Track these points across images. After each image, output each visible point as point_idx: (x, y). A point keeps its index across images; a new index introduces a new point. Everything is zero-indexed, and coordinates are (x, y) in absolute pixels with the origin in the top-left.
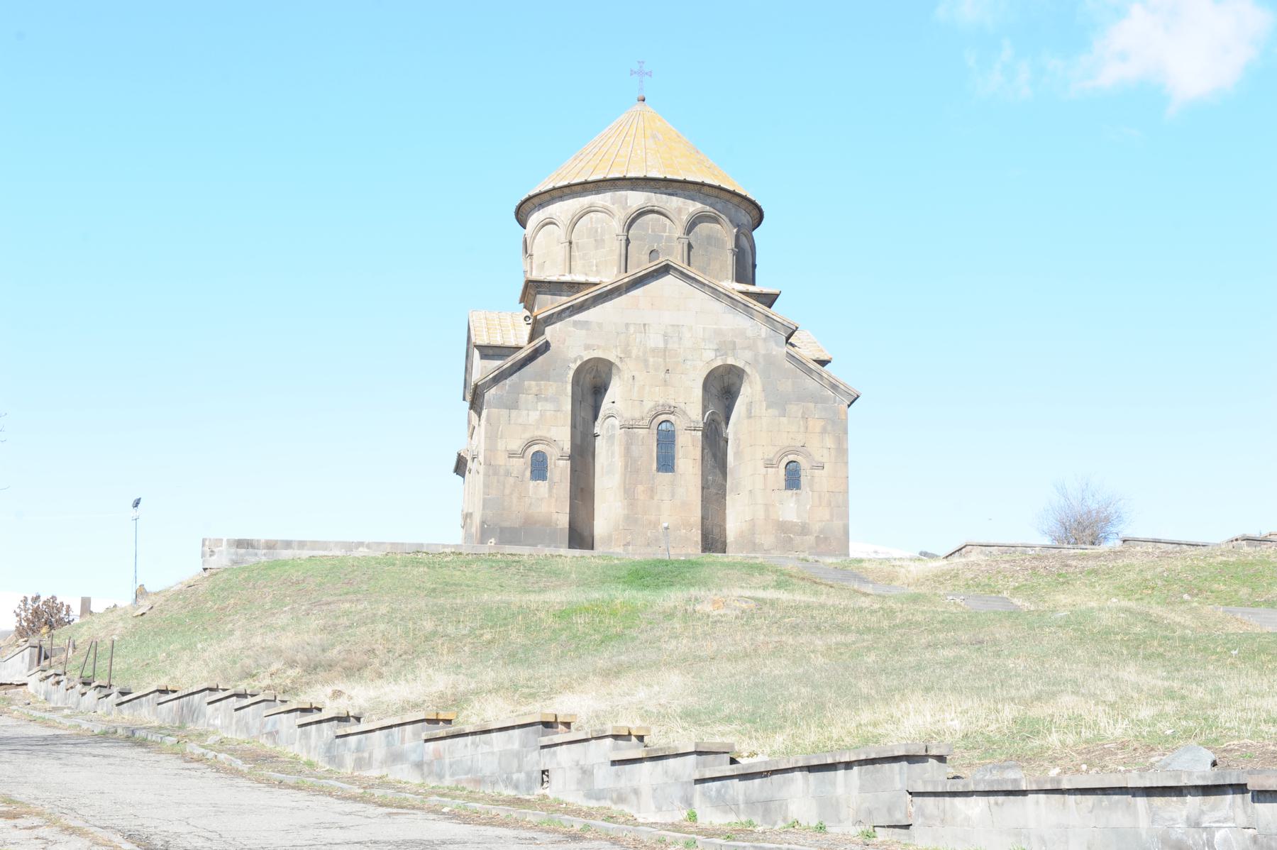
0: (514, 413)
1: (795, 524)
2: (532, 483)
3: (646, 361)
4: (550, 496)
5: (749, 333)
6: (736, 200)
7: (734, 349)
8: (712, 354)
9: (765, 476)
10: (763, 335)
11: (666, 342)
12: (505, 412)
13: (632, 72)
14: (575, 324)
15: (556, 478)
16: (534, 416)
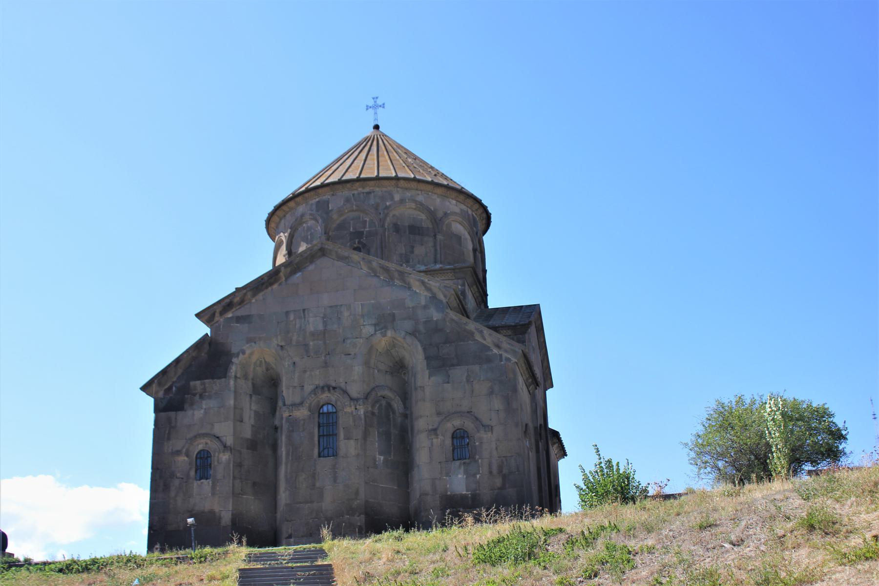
0: (180, 414)
1: (463, 497)
2: (196, 484)
3: (306, 345)
4: (213, 494)
5: (409, 303)
6: (439, 191)
7: (394, 320)
8: (370, 330)
9: (431, 450)
10: (423, 303)
11: (325, 324)
12: (172, 414)
13: (368, 107)
15: (219, 476)
16: (198, 414)
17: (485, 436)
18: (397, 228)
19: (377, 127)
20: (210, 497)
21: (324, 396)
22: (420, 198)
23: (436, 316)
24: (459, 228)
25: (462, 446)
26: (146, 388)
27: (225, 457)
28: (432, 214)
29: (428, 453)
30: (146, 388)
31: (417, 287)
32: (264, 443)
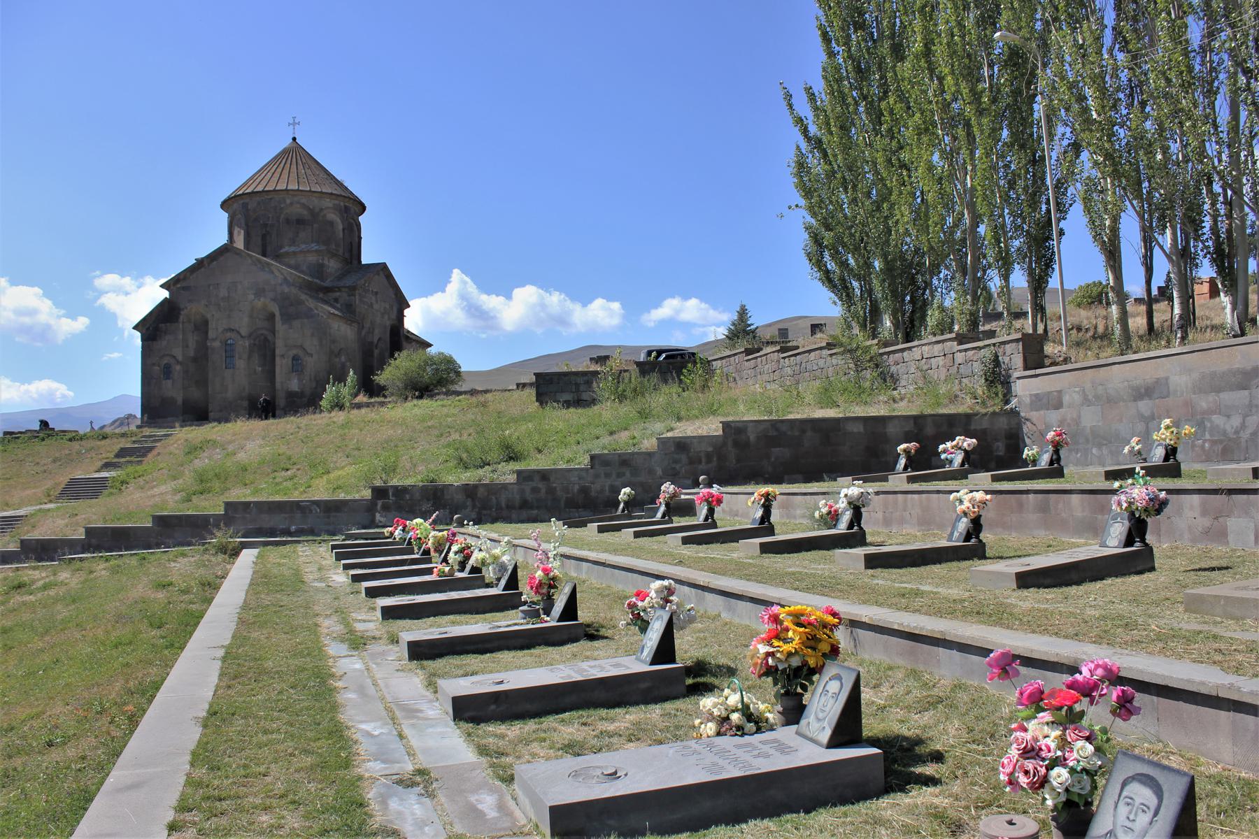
14: (184, 288)
16: (164, 343)
17: (309, 359)
18: (288, 221)
19: (294, 139)
20: (173, 390)
21: (229, 335)
22: (304, 201)
23: (286, 290)
24: (332, 216)
25: (297, 365)
26: (135, 328)
27: (178, 368)
28: (311, 211)
29: (282, 365)
30: (135, 328)
31: (277, 274)
32: (201, 358)
